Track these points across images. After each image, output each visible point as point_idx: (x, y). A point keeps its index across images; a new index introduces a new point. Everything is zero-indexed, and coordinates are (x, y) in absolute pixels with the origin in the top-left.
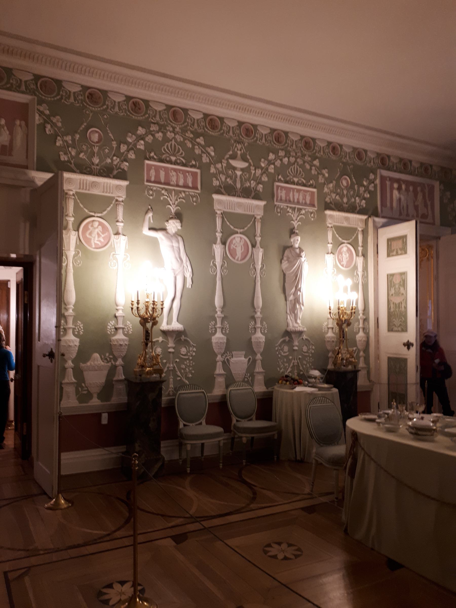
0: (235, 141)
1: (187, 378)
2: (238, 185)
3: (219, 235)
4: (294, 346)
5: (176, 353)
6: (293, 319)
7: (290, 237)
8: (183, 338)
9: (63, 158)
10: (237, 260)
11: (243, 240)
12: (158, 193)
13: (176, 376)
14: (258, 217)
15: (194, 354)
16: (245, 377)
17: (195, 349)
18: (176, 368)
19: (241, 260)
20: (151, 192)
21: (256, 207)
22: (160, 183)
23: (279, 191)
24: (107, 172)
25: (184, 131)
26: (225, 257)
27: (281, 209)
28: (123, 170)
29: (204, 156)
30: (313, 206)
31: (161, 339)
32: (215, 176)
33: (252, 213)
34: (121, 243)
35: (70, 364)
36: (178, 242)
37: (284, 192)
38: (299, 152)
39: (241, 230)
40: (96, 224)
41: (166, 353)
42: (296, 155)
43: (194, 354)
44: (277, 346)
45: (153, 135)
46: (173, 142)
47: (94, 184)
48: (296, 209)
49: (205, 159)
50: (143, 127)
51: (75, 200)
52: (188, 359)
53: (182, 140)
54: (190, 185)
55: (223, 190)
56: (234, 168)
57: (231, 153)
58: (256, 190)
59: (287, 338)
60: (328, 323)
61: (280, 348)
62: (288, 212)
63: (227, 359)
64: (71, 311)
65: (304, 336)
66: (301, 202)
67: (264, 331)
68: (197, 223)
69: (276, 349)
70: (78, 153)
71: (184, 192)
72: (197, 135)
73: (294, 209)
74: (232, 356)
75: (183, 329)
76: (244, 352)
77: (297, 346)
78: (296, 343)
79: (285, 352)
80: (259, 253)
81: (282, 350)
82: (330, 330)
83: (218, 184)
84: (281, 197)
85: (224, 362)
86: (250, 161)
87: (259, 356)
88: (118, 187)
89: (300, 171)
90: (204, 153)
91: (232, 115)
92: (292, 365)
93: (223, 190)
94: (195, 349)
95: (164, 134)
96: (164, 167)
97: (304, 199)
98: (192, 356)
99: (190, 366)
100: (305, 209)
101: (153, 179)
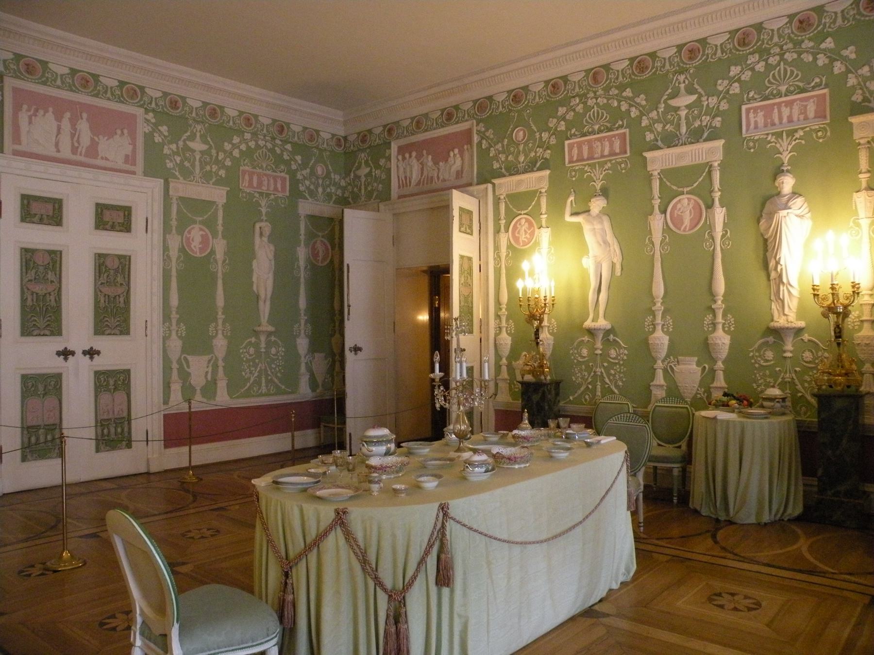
0: (675, 72)
1: (617, 386)
2: (684, 129)
3: (657, 202)
4: (785, 352)
5: (605, 356)
6: (780, 309)
7: (775, 179)
8: (611, 337)
9: (496, 166)
10: (684, 231)
11: (692, 201)
12: (582, 171)
13: (603, 382)
14: (716, 164)
15: (625, 358)
16: (697, 393)
17: (626, 352)
18: (605, 375)
19: (690, 230)
20: (573, 173)
21: (712, 151)
22: (583, 160)
23: (751, 115)
24: (531, 167)
25: (607, 89)
26: (667, 229)
27: (754, 141)
28: (546, 159)
29: (633, 109)
30: (825, 117)
31: (586, 338)
32: (650, 128)
33: (705, 161)
34: (545, 235)
35: (504, 361)
36: (601, 222)
37: (761, 114)
38: (786, 44)
39: (688, 189)
40: (523, 221)
41: (593, 355)
42: (782, 49)
43: (625, 358)
44: (752, 351)
45: (574, 110)
46: (596, 108)
47: (519, 183)
48: (784, 134)
49: (634, 113)
50: (562, 106)
51: (506, 202)
52: (618, 363)
53: (605, 101)
54: (618, 151)
55: (660, 143)
56: (677, 109)
57: (670, 91)
58: (711, 127)
59: (771, 339)
60: (862, 312)
61: (757, 354)
62: (770, 142)
63: (671, 367)
64: (504, 310)
65: (806, 335)
66: (795, 119)
67: (729, 327)
68: (627, 195)
69: (751, 354)
70: (507, 157)
71: (610, 161)
72: (622, 88)
73: (779, 135)
74: (678, 362)
75: (609, 327)
76: (696, 359)
77: (791, 352)
78: (789, 346)
79: (767, 361)
80: (720, 214)
81: (762, 357)
82: (866, 325)
83: (652, 137)
84: (756, 122)
85: (665, 371)
86: (700, 90)
87: (720, 365)
88: (541, 179)
89: (792, 72)
90: (633, 106)
91: (664, 43)
92: (780, 380)
93: (660, 143)
94: (626, 352)
95: (585, 103)
96: (586, 141)
97: (804, 111)
98: (623, 360)
99: (620, 372)
100: (802, 129)
101: (585, 157)
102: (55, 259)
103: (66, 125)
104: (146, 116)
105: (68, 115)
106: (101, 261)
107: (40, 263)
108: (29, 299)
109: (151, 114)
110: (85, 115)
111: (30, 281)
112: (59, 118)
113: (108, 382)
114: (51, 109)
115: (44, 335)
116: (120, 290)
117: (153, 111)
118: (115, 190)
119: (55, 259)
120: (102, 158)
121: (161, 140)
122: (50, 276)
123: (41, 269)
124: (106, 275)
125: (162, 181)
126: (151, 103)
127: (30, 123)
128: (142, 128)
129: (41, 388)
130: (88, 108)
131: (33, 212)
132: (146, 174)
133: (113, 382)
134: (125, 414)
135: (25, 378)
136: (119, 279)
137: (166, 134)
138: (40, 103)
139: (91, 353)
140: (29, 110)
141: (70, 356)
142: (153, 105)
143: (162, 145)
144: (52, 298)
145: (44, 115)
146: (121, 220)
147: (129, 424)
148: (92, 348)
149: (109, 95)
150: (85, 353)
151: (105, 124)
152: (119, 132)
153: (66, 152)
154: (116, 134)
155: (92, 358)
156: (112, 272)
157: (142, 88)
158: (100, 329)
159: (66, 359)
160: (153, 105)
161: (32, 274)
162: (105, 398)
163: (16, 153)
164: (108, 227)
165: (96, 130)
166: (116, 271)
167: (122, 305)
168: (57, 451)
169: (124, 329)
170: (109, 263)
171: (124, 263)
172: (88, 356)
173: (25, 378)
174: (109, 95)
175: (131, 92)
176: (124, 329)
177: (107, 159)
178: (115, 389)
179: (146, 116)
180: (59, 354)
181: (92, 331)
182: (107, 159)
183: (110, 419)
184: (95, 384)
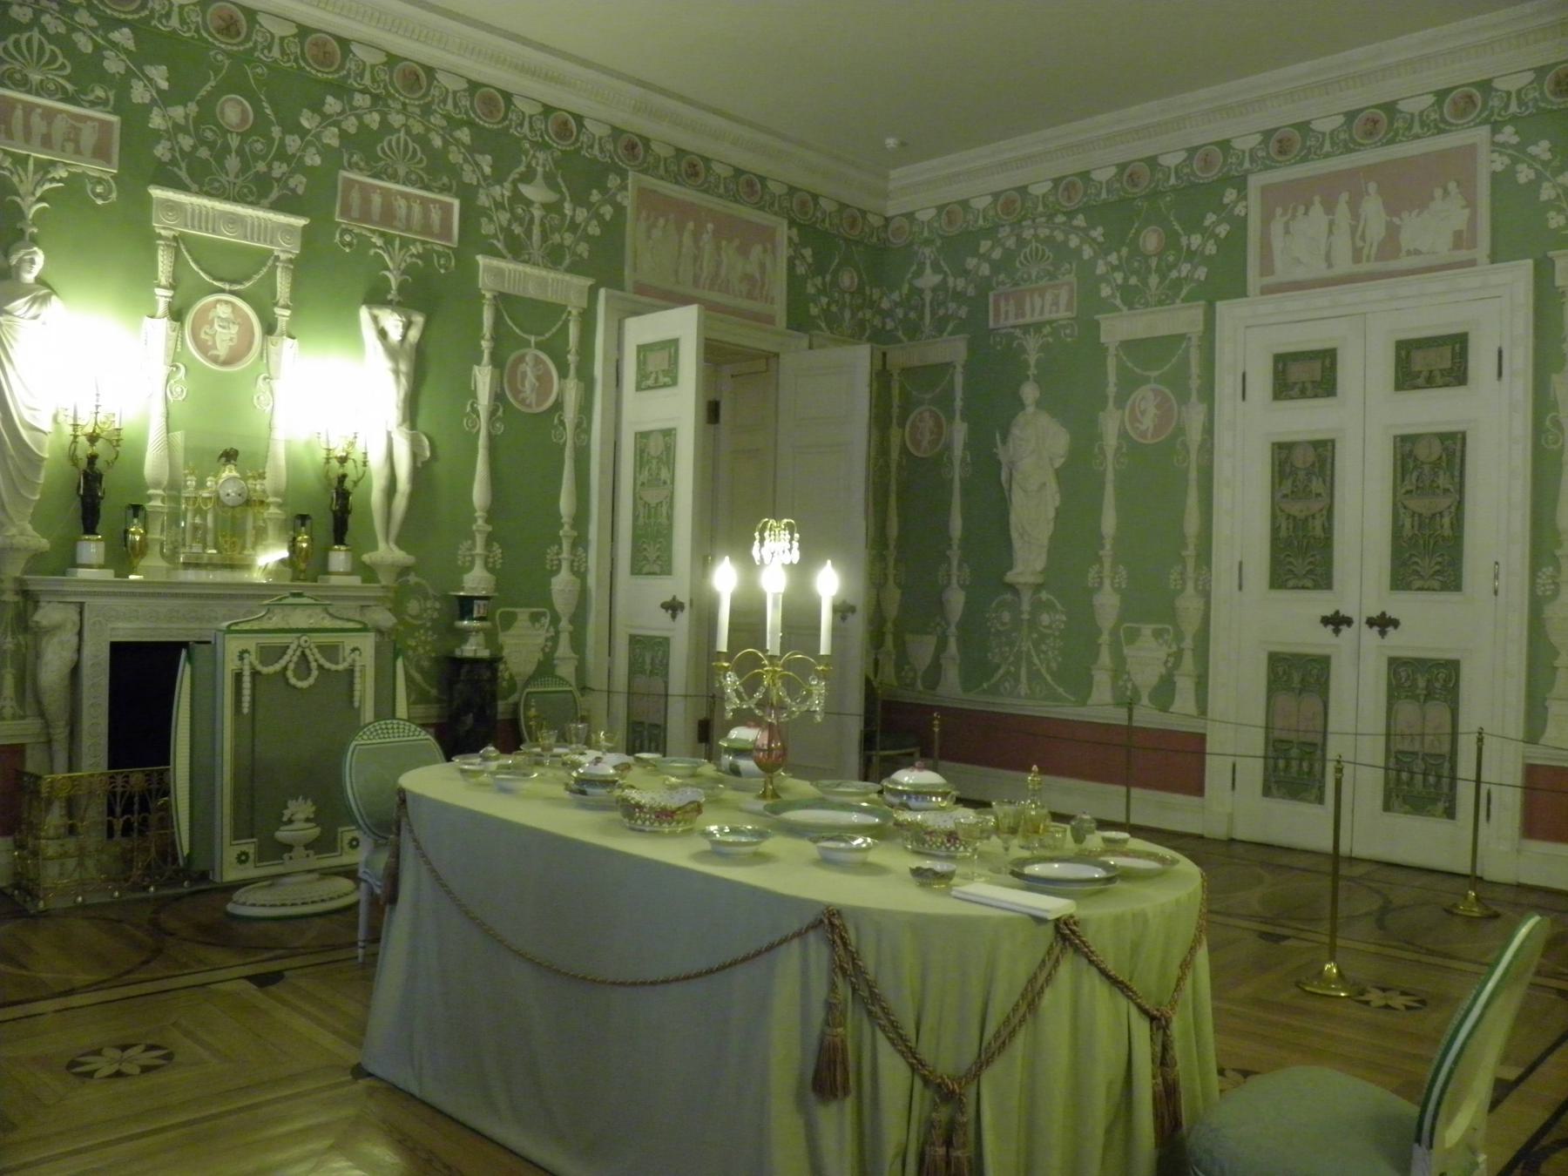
102: (1324, 452)
103: (1342, 209)
104: (1500, 138)
105: (1344, 197)
106: (1406, 450)
107: (1299, 464)
108: (1284, 526)
109: (1509, 129)
110: (1372, 187)
111: (1285, 496)
112: (1329, 209)
113: (1415, 680)
114: (1317, 199)
115: (1303, 588)
116: (1443, 503)
117: (1514, 119)
118: (1426, 310)
119: (1324, 452)
120: (1409, 253)
121: (1532, 175)
122: (1316, 485)
123: (1301, 475)
124: (1415, 474)
125: (1530, 262)
126: (1507, 106)
127: (1287, 232)
128: (1490, 163)
129: (1296, 678)
130: (1370, 171)
131: (1292, 378)
132: (1494, 258)
133: (1426, 682)
134: (1446, 749)
135: (1275, 659)
136: (1443, 481)
137: (1547, 156)
138: (1291, 197)
139: (1383, 623)
140: (1284, 213)
141: (1344, 628)
142: (1513, 108)
143: (1535, 185)
144: (1318, 523)
145: (1306, 213)
146: (1447, 364)
147: (1453, 769)
148: (1383, 614)
149: (1417, 129)
150: (1371, 622)
151: (1407, 189)
152: (1438, 192)
153: (1344, 265)
154: (1432, 198)
155: (1383, 633)
156: (1427, 468)
157: (1486, 86)
158: (1402, 577)
159: (1337, 631)
160: (1513, 108)
161: (1287, 487)
162: (1408, 711)
163: (1266, 290)
164: (1421, 381)
165: (1393, 209)
166: (1436, 465)
167: (1447, 532)
168: (1315, 791)
169: (1449, 577)
170: (1422, 452)
171: (1453, 448)
172: (1376, 629)
173: (1275, 659)
174: (1417, 129)
175: (1466, 102)
176: (1449, 577)
177: (1417, 252)
178: (1429, 696)
179: (1500, 138)
180: (1326, 621)
181: (1386, 578)
182: (1417, 252)
183: (1415, 754)
184: (1389, 684)
